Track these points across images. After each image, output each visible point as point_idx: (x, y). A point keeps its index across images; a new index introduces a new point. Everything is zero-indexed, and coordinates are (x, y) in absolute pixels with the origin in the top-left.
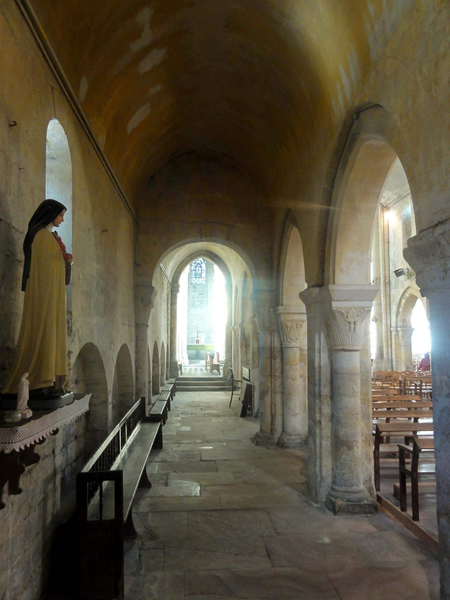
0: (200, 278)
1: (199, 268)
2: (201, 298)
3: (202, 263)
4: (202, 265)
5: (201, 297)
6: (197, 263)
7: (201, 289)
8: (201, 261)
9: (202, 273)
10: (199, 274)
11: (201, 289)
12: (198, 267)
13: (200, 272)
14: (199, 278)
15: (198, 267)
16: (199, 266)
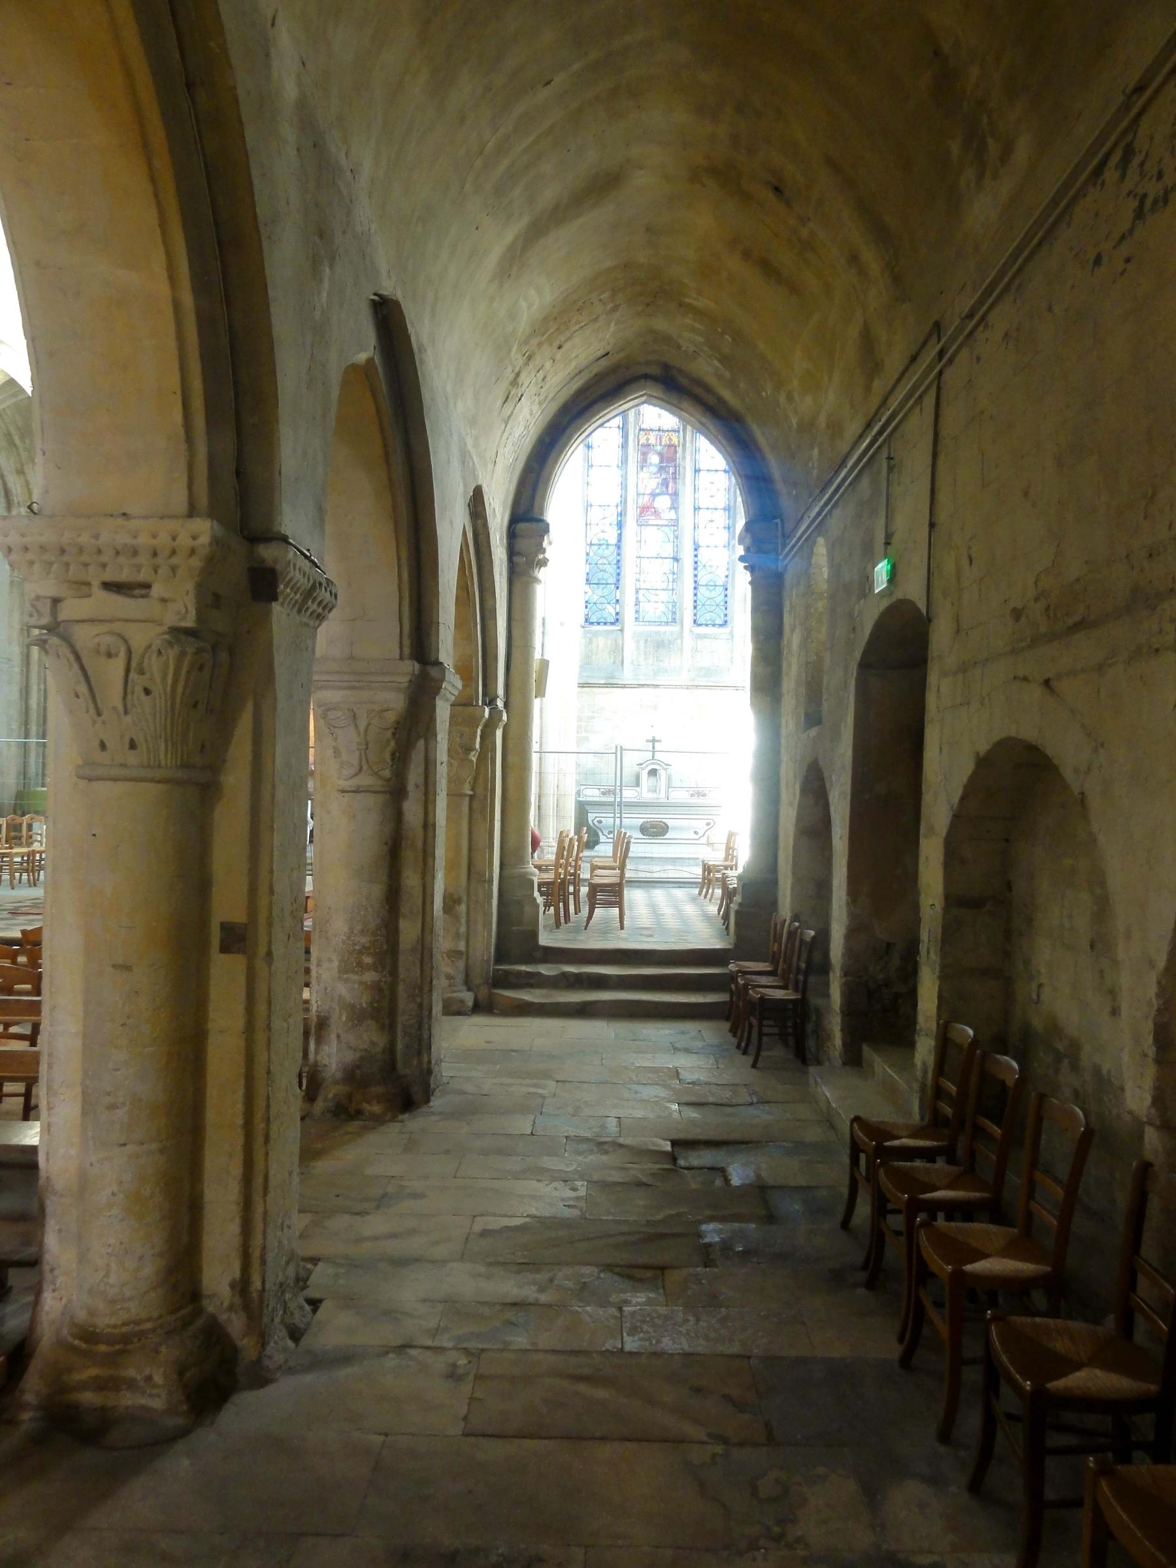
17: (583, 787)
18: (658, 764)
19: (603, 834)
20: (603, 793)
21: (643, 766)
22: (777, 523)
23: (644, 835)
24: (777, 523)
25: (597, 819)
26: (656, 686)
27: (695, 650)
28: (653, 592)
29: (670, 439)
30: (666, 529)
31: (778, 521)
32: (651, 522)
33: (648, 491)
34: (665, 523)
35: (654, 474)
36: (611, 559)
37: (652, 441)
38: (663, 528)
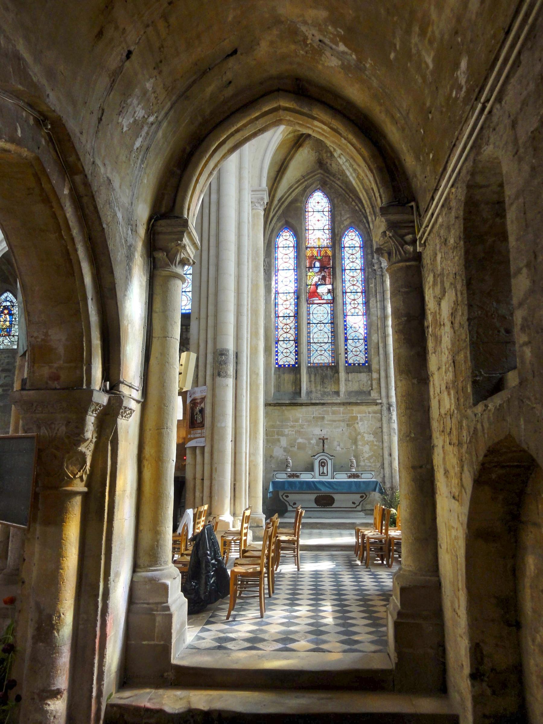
0: (7, 337)
1: (8, 316)
2: (4, 379)
3: (13, 306)
4: (12, 309)
5: (5, 377)
6: (4, 306)
7: (8, 360)
8: (11, 302)
9: (12, 326)
10: (5, 329)
11: (6, 361)
12: (5, 314)
13: (8, 323)
14: (5, 336)
15: (5, 314)
16: (6, 312)
17: (276, 473)
18: (326, 456)
19: (290, 505)
20: (289, 477)
21: (316, 457)
22: (412, 207)
23: (318, 505)
24: (412, 207)
25: (285, 494)
26: (323, 404)
27: (347, 380)
28: (318, 344)
29: (326, 252)
30: (326, 305)
31: (413, 204)
32: (316, 302)
33: (313, 282)
34: (325, 301)
35: (316, 273)
36: (291, 325)
37: (315, 254)
38: (323, 305)
